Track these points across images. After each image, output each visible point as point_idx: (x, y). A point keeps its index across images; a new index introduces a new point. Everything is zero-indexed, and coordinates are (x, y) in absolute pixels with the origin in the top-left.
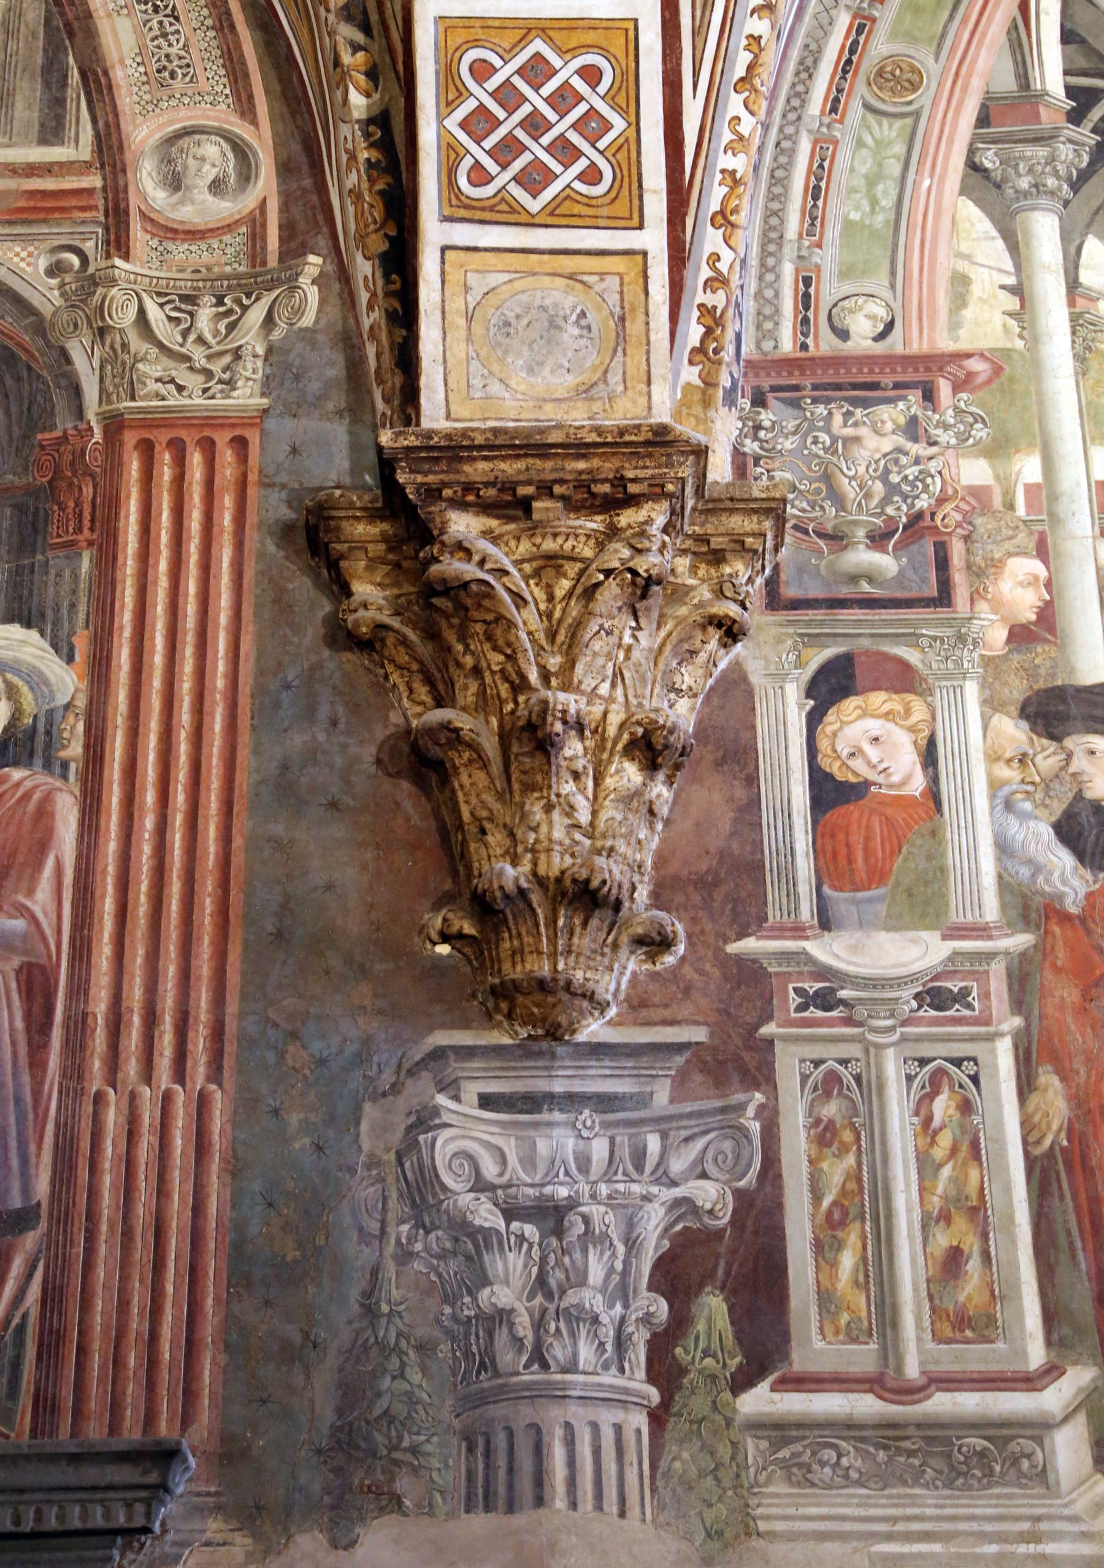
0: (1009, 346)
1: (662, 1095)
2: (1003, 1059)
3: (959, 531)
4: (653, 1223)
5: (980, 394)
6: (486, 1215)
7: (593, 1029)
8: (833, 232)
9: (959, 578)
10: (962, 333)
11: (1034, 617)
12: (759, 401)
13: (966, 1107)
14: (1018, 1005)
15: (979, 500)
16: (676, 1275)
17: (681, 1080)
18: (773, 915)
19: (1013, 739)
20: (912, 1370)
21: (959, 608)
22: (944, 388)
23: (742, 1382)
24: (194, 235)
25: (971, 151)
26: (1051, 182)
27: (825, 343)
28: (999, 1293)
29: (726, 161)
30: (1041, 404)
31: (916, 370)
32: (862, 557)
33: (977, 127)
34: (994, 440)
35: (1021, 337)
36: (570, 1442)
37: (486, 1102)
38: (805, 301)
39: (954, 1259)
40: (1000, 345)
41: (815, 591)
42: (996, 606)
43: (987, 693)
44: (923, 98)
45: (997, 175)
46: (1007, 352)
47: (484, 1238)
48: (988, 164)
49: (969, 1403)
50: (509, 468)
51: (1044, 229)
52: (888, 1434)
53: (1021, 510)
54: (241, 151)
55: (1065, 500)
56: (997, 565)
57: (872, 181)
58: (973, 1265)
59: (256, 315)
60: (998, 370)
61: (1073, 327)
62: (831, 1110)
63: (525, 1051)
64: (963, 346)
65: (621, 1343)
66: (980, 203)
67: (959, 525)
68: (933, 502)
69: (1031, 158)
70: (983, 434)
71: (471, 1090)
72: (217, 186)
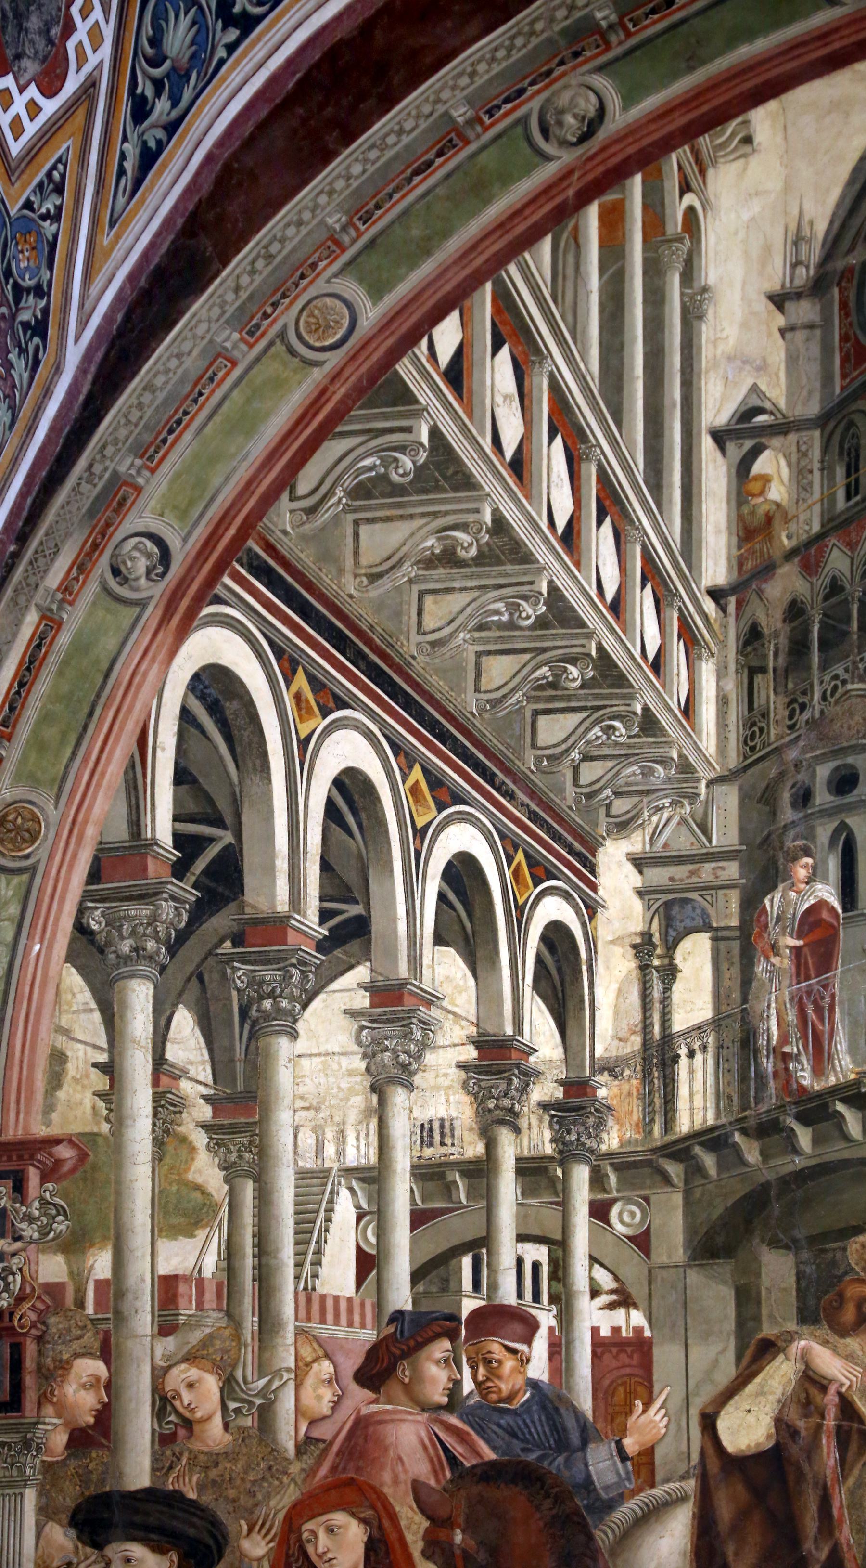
0: (95, 1130)
3: (33, 1331)
5: (65, 1184)
9: (29, 1381)
10: (54, 1116)
11: (91, 1420)
15: (53, 1298)
19: (62, 1548)
21: (27, 1413)
22: (33, 1176)
25: (81, 911)
26: (151, 945)
30: (118, 1193)
31: (10, 1159)
33: (88, 883)
34: (73, 1233)
35: (107, 1120)
40: (87, 1129)
42: (61, 1409)
43: (44, 1500)
44: (39, 850)
45: (101, 938)
48: (94, 926)
53: (90, 1309)
55: (130, 1296)
56: (64, 1366)
60: (83, 1157)
61: (155, 1108)
64: (55, 1131)
66: (83, 971)
67: (34, 1325)
68: (12, 1301)
69: (134, 918)
70: (63, 1227)
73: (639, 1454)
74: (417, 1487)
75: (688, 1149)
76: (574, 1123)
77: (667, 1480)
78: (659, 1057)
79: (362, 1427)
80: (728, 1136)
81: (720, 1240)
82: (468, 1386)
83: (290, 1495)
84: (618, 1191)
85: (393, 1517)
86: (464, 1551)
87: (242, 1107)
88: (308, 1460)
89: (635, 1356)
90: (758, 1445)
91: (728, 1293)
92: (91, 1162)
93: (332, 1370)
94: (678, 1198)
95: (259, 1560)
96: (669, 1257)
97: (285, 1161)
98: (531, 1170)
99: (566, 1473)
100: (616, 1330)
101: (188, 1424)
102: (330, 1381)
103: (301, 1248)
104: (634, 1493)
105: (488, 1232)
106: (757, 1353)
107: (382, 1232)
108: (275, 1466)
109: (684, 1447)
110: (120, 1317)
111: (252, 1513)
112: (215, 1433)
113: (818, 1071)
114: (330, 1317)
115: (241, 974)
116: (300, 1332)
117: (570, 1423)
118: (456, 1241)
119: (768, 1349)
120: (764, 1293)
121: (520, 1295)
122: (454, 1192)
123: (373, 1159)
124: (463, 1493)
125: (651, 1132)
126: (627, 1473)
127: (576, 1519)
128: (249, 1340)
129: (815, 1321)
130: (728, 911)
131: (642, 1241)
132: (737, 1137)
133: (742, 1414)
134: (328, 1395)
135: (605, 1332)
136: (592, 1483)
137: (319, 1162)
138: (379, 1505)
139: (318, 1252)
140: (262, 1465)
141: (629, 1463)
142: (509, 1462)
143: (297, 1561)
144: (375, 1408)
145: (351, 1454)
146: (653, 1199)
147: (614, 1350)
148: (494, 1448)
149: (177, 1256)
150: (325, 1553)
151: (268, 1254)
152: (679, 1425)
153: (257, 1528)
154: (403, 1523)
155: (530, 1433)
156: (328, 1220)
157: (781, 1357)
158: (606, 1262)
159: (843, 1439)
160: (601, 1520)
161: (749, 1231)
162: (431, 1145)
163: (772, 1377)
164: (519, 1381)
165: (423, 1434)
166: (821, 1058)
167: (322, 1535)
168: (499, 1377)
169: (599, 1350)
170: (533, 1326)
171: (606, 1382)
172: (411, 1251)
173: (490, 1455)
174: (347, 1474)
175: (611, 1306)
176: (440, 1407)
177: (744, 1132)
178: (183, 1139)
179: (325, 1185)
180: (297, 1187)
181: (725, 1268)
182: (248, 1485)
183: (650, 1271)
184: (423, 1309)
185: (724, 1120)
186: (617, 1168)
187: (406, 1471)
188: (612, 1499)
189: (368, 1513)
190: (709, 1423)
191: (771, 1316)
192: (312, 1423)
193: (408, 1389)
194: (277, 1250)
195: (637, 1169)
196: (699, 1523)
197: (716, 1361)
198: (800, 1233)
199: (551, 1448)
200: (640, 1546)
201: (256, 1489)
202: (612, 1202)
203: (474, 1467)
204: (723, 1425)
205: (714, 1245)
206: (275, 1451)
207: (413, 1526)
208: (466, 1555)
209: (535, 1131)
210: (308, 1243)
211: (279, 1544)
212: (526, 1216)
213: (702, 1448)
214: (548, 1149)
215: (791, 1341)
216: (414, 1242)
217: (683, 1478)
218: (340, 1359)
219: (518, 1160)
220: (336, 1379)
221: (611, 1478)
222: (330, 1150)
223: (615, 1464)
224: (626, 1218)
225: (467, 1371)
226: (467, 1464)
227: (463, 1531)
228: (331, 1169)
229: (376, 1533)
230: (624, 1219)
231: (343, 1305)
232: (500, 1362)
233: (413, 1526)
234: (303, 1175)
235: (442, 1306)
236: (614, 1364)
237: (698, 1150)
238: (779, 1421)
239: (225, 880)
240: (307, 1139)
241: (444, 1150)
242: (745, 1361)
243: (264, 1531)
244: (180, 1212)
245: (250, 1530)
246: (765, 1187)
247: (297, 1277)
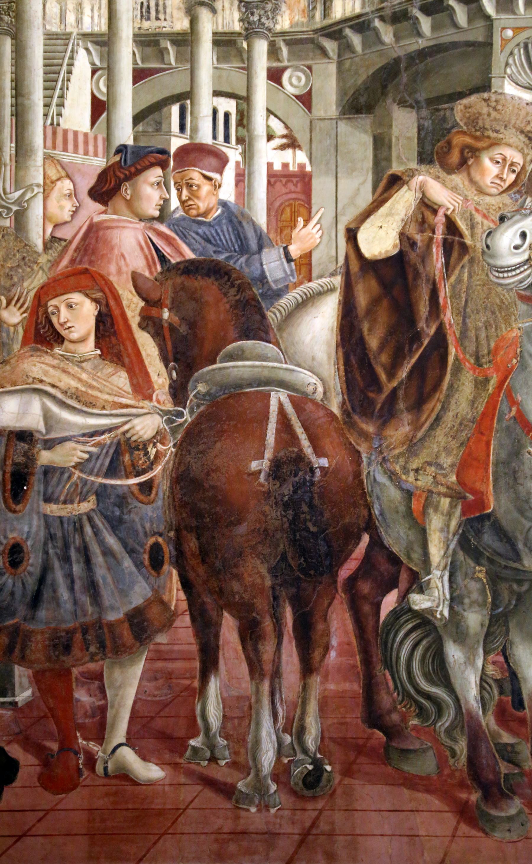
73: (301, 257)
74: (135, 277)
75: (341, 31)
76: (257, 7)
77: (321, 277)
79: (94, 230)
80: (370, 22)
81: (362, 100)
82: (175, 203)
83: (39, 279)
84: (289, 61)
85: (117, 299)
86: (170, 325)
88: (53, 254)
89: (299, 185)
90: (387, 251)
91: (368, 140)
93: (72, 187)
94: (333, 68)
95: (15, 326)
96: (326, 111)
97: (36, 24)
98: (224, 42)
99: (247, 270)
100: (285, 166)
102: (70, 195)
103: (49, 92)
104: (296, 285)
105: (192, 88)
106: (389, 184)
107: (110, 84)
108: (28, 258)
109: (333, 253)
111: (9, 291)
114: (71, 147)
116: (47, 157)
117: (250, 234)
118: (166, 93)
119: (395, 182)
120: (394, 140)
121: (215, 137)
122: (166, 56)
123: (104, 28)
124: (170, 282)
125: (313, 17)
126: (292, 271)
127: (253, 303)
128: (8, 161)
129: (431, 162)
131: (306, 100)
132: (377, 23)
133: (376, 229)
134: (68, 206)
135: (277, 167)
136: (266, 277)
137: (63, 27)
138: (107, 290)
139: (62, 96)
140: (18, 256)
141: (293, 264)
142: (205, 260)
143: (44, 328)
144: (104, 217)
145: (86, 250)
146: (314, 68)
147: (284, 180)
148: (193, 250)
150: (65, 323)
151: (23, 96)
152: (330, 236)
153: (14, 302)
154: (125, 303)
155: (221, 240)
156: (70, 72)
157: (405, 188)
158: (278, 114)
160: (272, 304)
161: (384, 94)
162: (148, 19)
163: (398, 202)
164: (213, 201)
165: (141, 238)
167: (63, 309)
168: (198, 198)
169: (272, 180)
170: (223, 161)
171: (277, 204)
172: (133, 99)
173: (190, 255)
174: (83, 265)
175: (283, 147)
176: (154, 219)
177: (382, 19)
179: (67, 45)
180: (45, 45)
182: (7, 270)
183: (311, 122)
184: (142, 144)
185: (367, 10)
186: (288, 43)
187: (127, 265)
188: (280, 290)
189: (99, 295)
190: (352, 235)
191: (399, 157)
192: (56, 226)
193: (129, 203)
194: (30, 93)
195: (304, 44)
196: (343, 308)
197: (358, 189)
198: (422, 96)
199: (235, 251)
200: (300, 324)
201: (13, 273)
202: (284, 69)
203: (178, 263)
204: (361, 237)
205: (359, 103)
206: (27, 246)
207: (132, 305)
208: (172, 328)
209: (227, 12)
210: (54, 89)
211: (31, 315)
212: (220, 77)
213: (347, 254)
214: (237, 27)
215: (412, 176)
216: (135, 93)
217: (332, 275)
218: (78, 179)
219: (215, 34)
220: (74, 194)
221: (280, 274)
222: (71, 18)
223: (282, 264)
224: (294, 81)
225: (174, 192)
226: (173, 261)
227: (170, 310)
228: (70, 34)
229: (104, 309)
230: (293, 82)
231: (81, 139)
232: (199, 186)
233: (132, 305)
234: (50, 37)
235: (156, 143)
236: (284, 190)
237: (348, 32)
238: (402, 235)
241: (158, 23)
242: (380, 190)
243: (19, 305)
245: (8, 304)
246: (397, 61)
247: (46, 115)
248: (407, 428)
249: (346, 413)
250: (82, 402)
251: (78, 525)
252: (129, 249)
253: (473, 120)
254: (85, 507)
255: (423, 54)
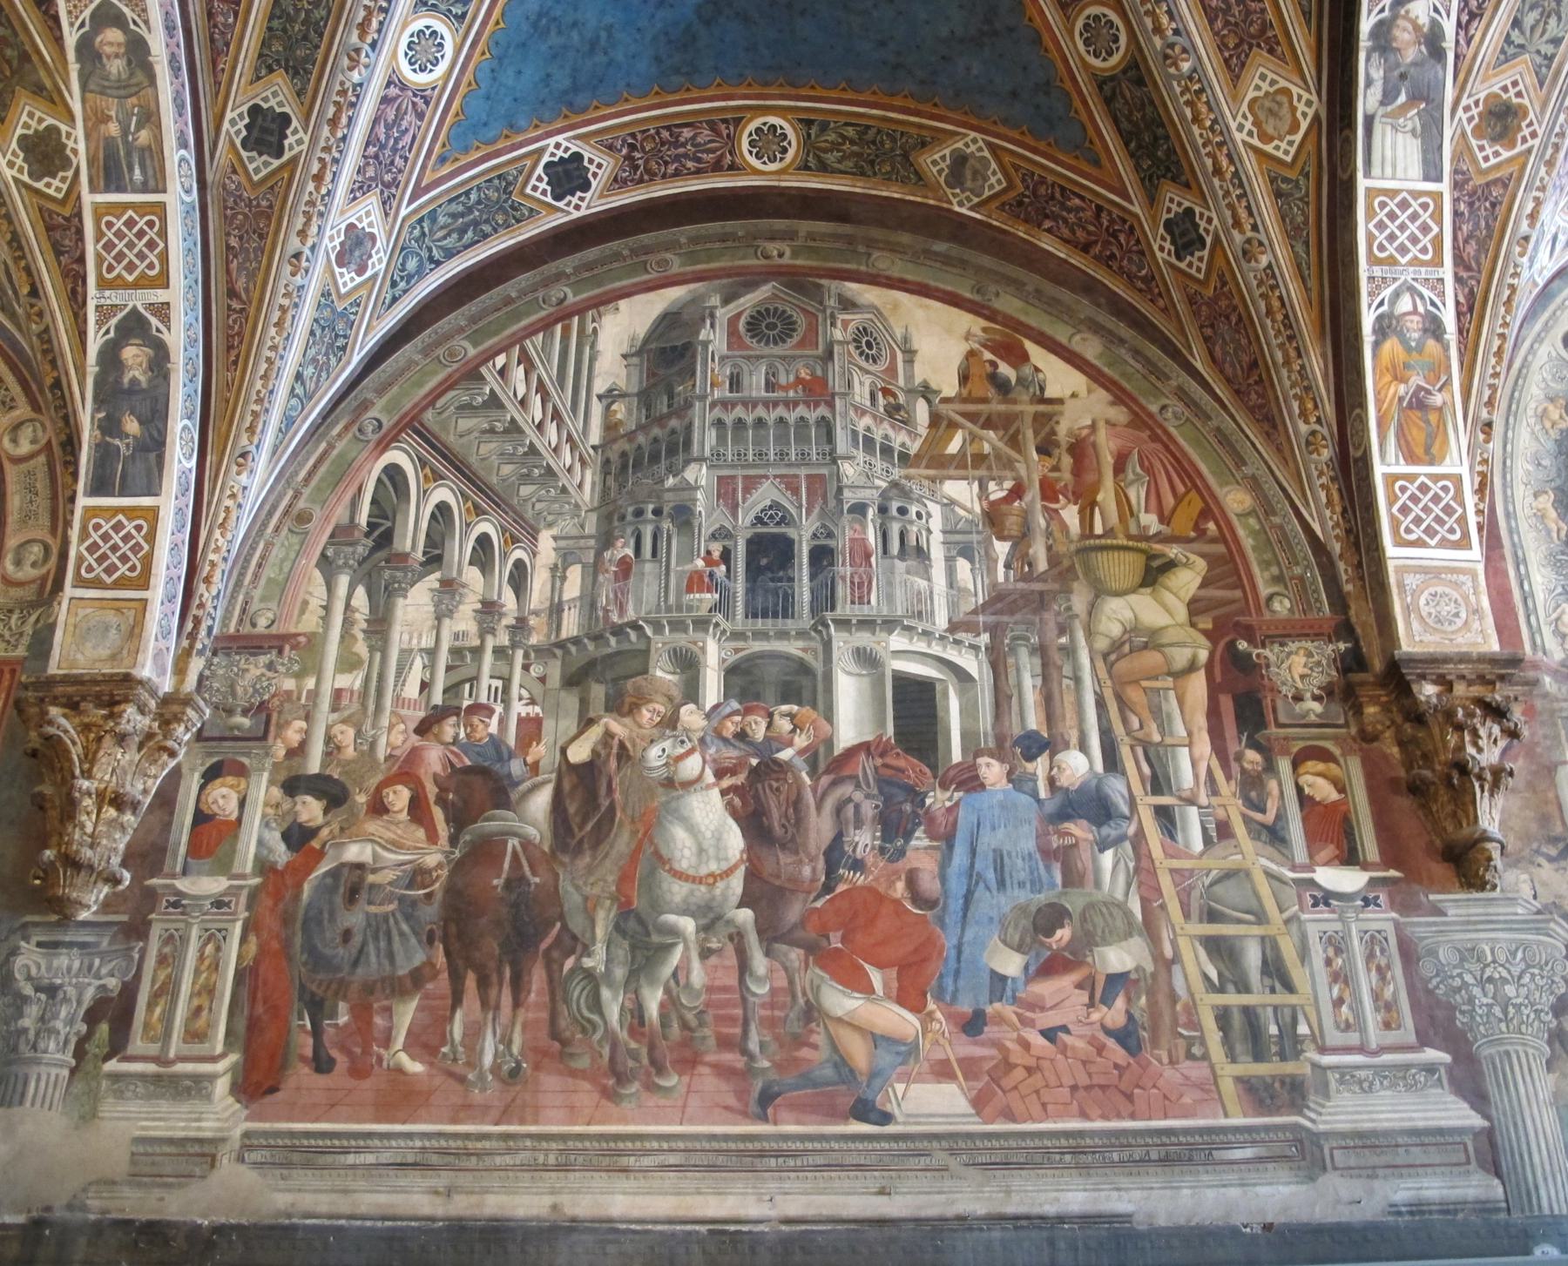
1: (105, 943)
2: (238, 929)
4: (89, 994)
6: (28, 990)
7: (84, 915)
8: (263, 582)
12: (215, 653)
13: (218, 949)
14: (249, 907)
16: (92, 1017)
17: (114, 937)
18: (166, 869)
20: (172, 1054)
23: (107, 1058)
24: (20, 584)
27: (246, 629)
28: (212, 1025)
29: (212, 556)
32: (239, 720)
36: (38, 1080)
37: (39, 945)
38: (244, 611)
39: (199, 1009)
41: (216, 734)
46: (314, 634)
47: (25, 999)
49: (189, 1067)
50: (70, 689)
51: (343, 581)
52: (157, 1079)
54: (47, 549)
56: (288, 723)
57: (283, 561)
58: (205, 1013)
59: (33, 618)
62: (167, 950)
63: (58, 924)
65: (66, 1042)
71: (35, 939)
72: (34, 565)
74: (435, 775)
78: (556, 610)
83: (380, 777)
87: (380, 625)
92: (311, 646)
98: (499, 652)
101: (339, 748)
106: (586, 723)
110: (315, 705)
112: (350, 752)
113: (621, 615)
115: (387, 574)
130: (590, 557)
131: (542, 680)
149: (343, 681)
159: (619, 758)
166: (622, 610)
174: (406, 770)
178: (354, 637)
181: (576, 690)
190: (563, 751)
195: (543, 652)
205: (575, 680)
207: (432, 791)
230: (536, 670)
233: (432, 791)
235: (455, 703)
238: (594, 751)
239: (385, 539)
240: (406, 637)
244: (348, 663)
248: (587, 859)
249: (553, 851)
250: (396, 846)
251: (386, 918)
252: (434, 759)
253: (638, 689)
254: (391, 907)
255: (610, 656)
